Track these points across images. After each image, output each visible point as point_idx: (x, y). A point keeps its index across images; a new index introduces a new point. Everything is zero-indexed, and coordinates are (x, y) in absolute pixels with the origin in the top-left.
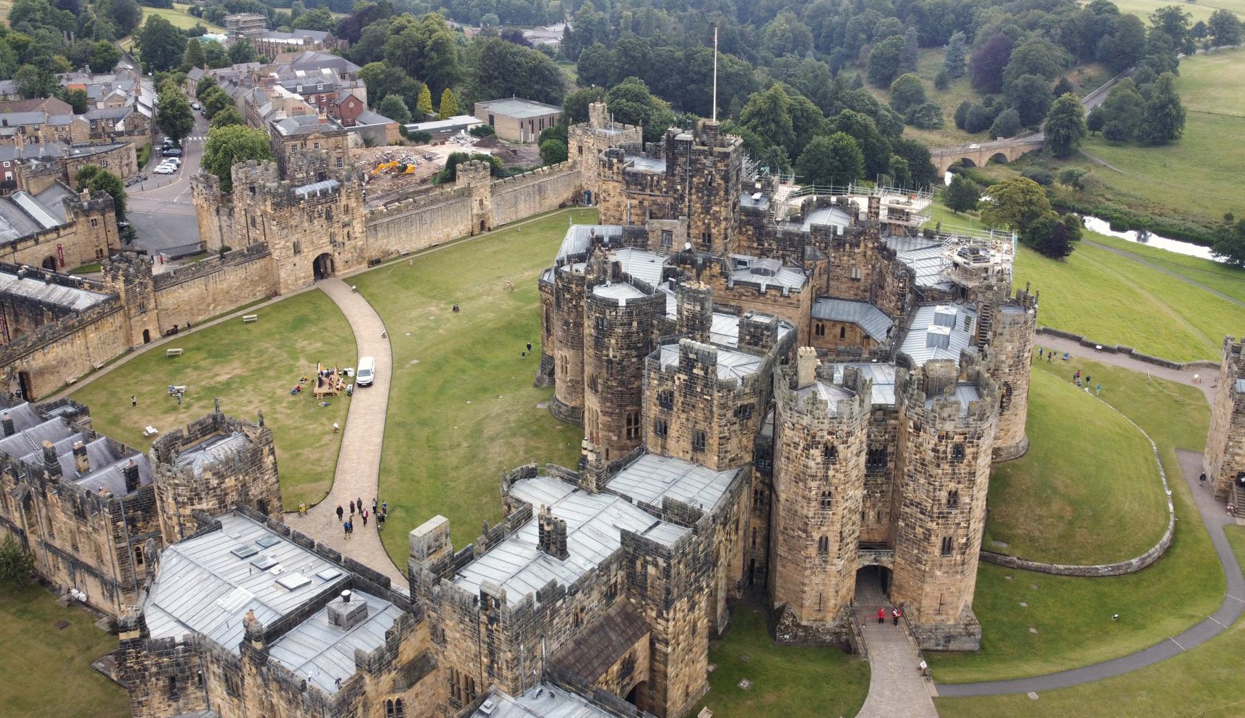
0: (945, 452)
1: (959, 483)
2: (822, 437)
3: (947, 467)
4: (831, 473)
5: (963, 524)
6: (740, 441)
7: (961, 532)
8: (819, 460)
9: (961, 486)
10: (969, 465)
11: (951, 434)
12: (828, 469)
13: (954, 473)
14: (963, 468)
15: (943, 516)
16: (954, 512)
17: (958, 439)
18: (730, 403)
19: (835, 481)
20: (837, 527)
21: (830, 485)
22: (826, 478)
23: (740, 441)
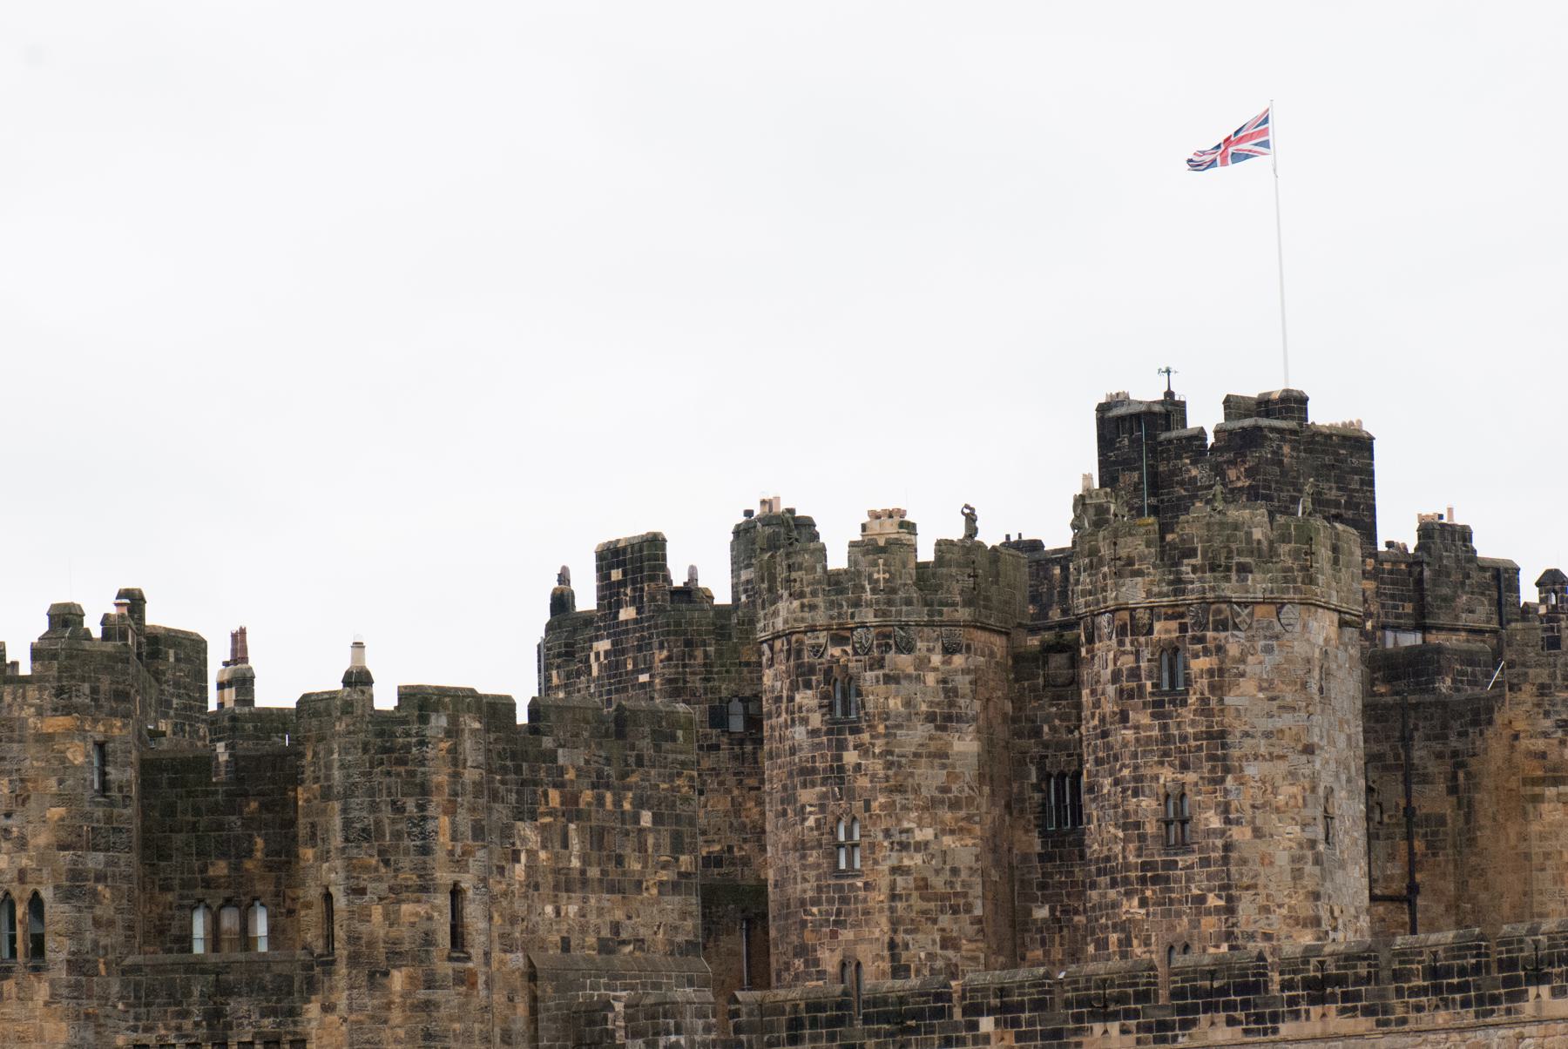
0: (1134, 673)
1: (1184, 767)
2: (818, 651)
3: (1145, 719)
4: (850, 757)
5: (1213, 901)
6: (737, 808)
7: (1210, 924)
8: (816, 720)
9: (1191, 777)
10: (1204, 709)
11: (1142, 616)
12: (842, 746)
13: (1167, 739)
14: (1187, 720)
15: (1155, 876)
16: (1182, 861)
17: (1164, 630)
18: (696, 682)
19: (863, 782)
20: (880, 929)
21: (850, 794)
22: (837, 773)
23: (737, 808)
